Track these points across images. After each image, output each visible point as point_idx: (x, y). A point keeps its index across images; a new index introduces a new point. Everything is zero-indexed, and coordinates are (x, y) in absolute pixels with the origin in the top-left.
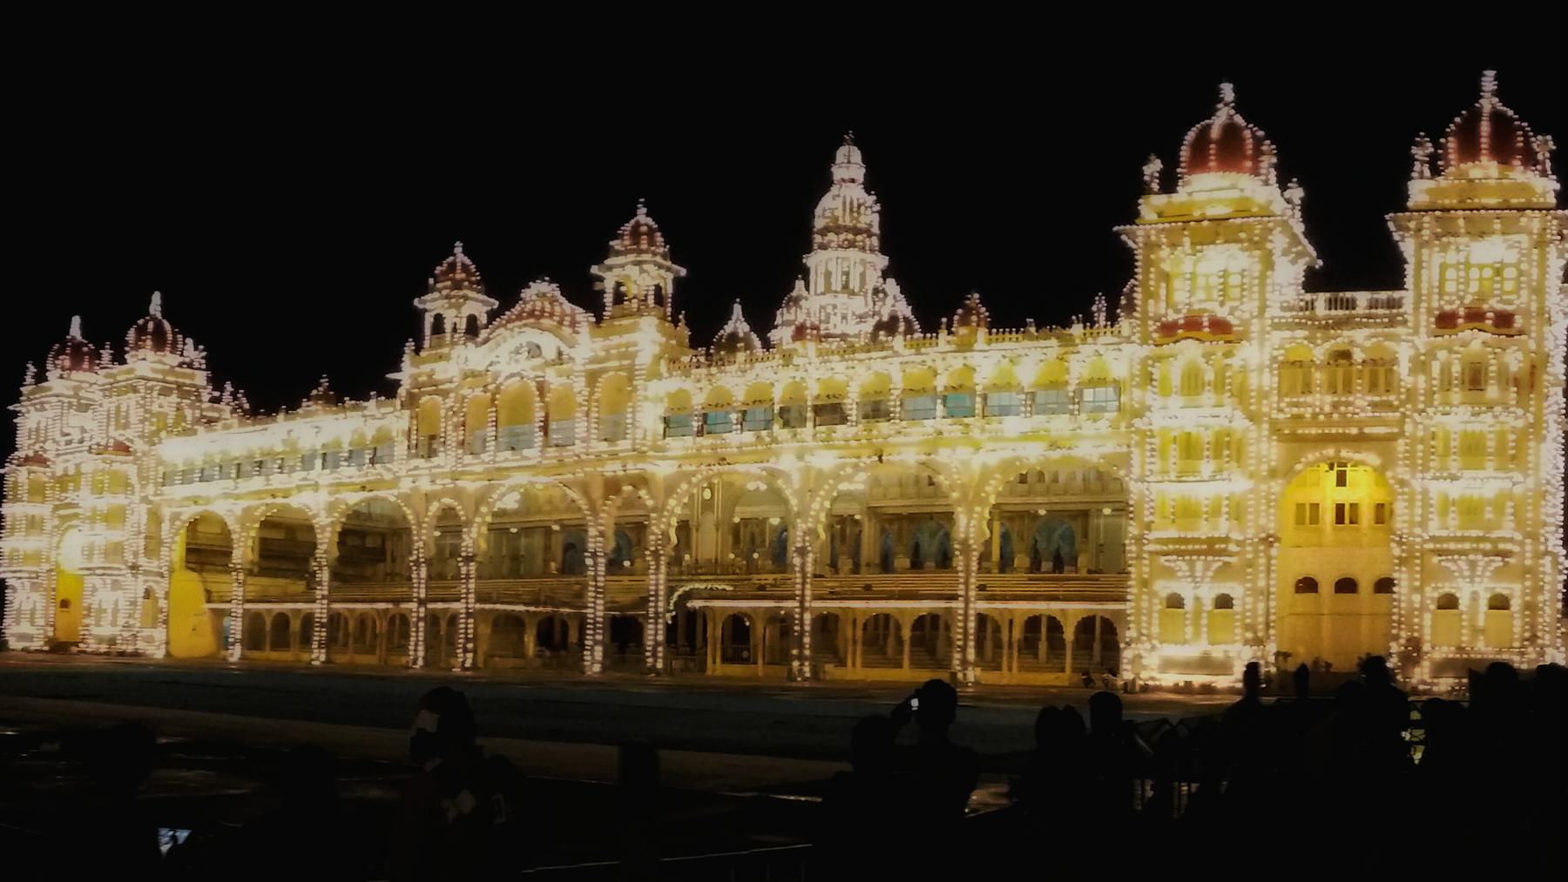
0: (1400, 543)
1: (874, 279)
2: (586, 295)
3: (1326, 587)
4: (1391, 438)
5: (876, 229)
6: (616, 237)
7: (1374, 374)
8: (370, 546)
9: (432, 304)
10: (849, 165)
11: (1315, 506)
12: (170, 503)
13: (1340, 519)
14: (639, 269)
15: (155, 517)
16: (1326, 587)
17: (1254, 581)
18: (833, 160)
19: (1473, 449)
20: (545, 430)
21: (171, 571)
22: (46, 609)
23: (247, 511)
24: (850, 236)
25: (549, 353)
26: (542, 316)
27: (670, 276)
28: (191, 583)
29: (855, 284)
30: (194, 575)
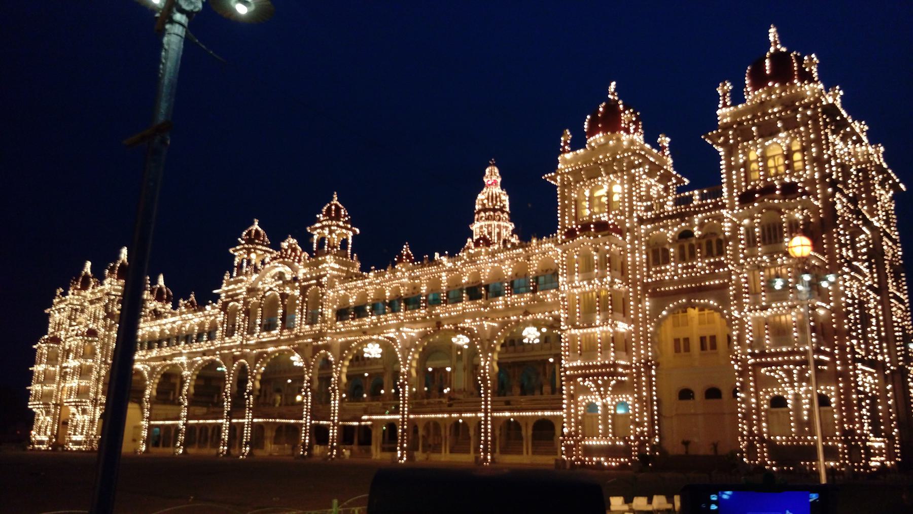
0: (736, 361)
4: (725, 286)
7: (709, 243)
9: (238, 255)
10: (492, 176)
11: (687, 340)
13: (703, 347)
14: (334, 229)
16: (699, 395)
17: (639, 392)
24: (492, 213)
25: (288, 277)
27: (351, 234)
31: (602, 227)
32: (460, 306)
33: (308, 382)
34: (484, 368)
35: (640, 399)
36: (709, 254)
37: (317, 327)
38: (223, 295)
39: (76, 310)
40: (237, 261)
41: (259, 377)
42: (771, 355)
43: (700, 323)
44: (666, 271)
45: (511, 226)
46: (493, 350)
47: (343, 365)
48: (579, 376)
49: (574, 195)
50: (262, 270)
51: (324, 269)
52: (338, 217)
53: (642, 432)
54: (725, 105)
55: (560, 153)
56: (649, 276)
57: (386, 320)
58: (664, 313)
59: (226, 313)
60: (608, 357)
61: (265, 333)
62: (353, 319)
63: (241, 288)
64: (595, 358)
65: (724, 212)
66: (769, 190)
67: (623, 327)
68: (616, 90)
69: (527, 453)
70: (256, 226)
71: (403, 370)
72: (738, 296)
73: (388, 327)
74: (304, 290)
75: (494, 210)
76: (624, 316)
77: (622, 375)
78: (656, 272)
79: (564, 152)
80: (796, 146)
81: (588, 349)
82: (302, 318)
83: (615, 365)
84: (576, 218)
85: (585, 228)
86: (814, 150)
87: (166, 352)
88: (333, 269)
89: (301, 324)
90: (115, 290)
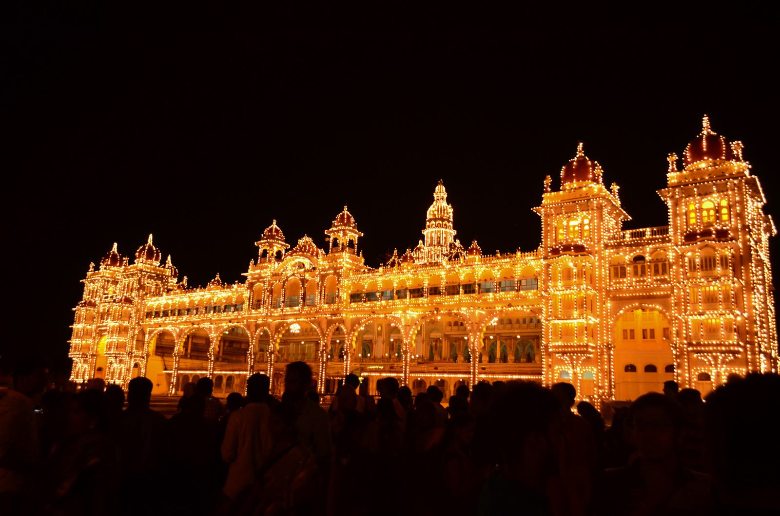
0: (675, 348)
1: (450, 240)
2: (322, 243)
3: (640, 369)
4: (668, 296)
6: (335, 219)
8: (233, 347)
9: (262, 246)
10: (440, 192)
11: (632, 331)
12: (150, 326)
14: (344, 232)
15: (143, 333)
16: (640, 369)
18: (434, 191)
19: (711, 300)
20: (304, 299)
21: (148, 355)
22: (90, 371)
23: (181, 330)
24: (441, 222)
26: (305, 251)
27: (357, 236)
28: (156, 362)
29: (442, 242)
30: (159, 358)
31: (579, 249)
32: (457, 297)
33: (324, 346)
34: (473, 343)
35: (602, 370)
36: (656, 272)
37: (334, 306)
38: (249, 277)
39: (108, 281)
40: (260, 251)
41: (278, 341)
42: (705, 345)
43: (643, 319)
44: (624, 282)
45: (454, 233)
46: (481, 331)
47: (354, 335)
48: (558, 353)
49: (555, 224)
51: (340, 263)
52: (348, 223)
53: (603, 393)
54: (673, 170)
55: (544, 192)
56: (610, 286)
57: (394, 304)
58: (621, 312)
60: (582, 340)
61: (288, 308)
62: (365, 302)
63: (266, 273)
64: (573, 341)
66: (706, 234)
67: (593, 320)
68: (583, 149)
70: (274, 226)
71: (405, 341)
73: (397, 309)
74: (323, 277)
75: (443, 220)
76: (592, 312)
77: (590, 353)
78: (616, 283)
79: (547, 191)
81: (567, 333)
82: (320, 299)
83: (587, 346)
84: (556, 240)
85: (567, 248)
86: (738, 208)
87: (195, 318)
88: (347, 263)
89: (320, 303)
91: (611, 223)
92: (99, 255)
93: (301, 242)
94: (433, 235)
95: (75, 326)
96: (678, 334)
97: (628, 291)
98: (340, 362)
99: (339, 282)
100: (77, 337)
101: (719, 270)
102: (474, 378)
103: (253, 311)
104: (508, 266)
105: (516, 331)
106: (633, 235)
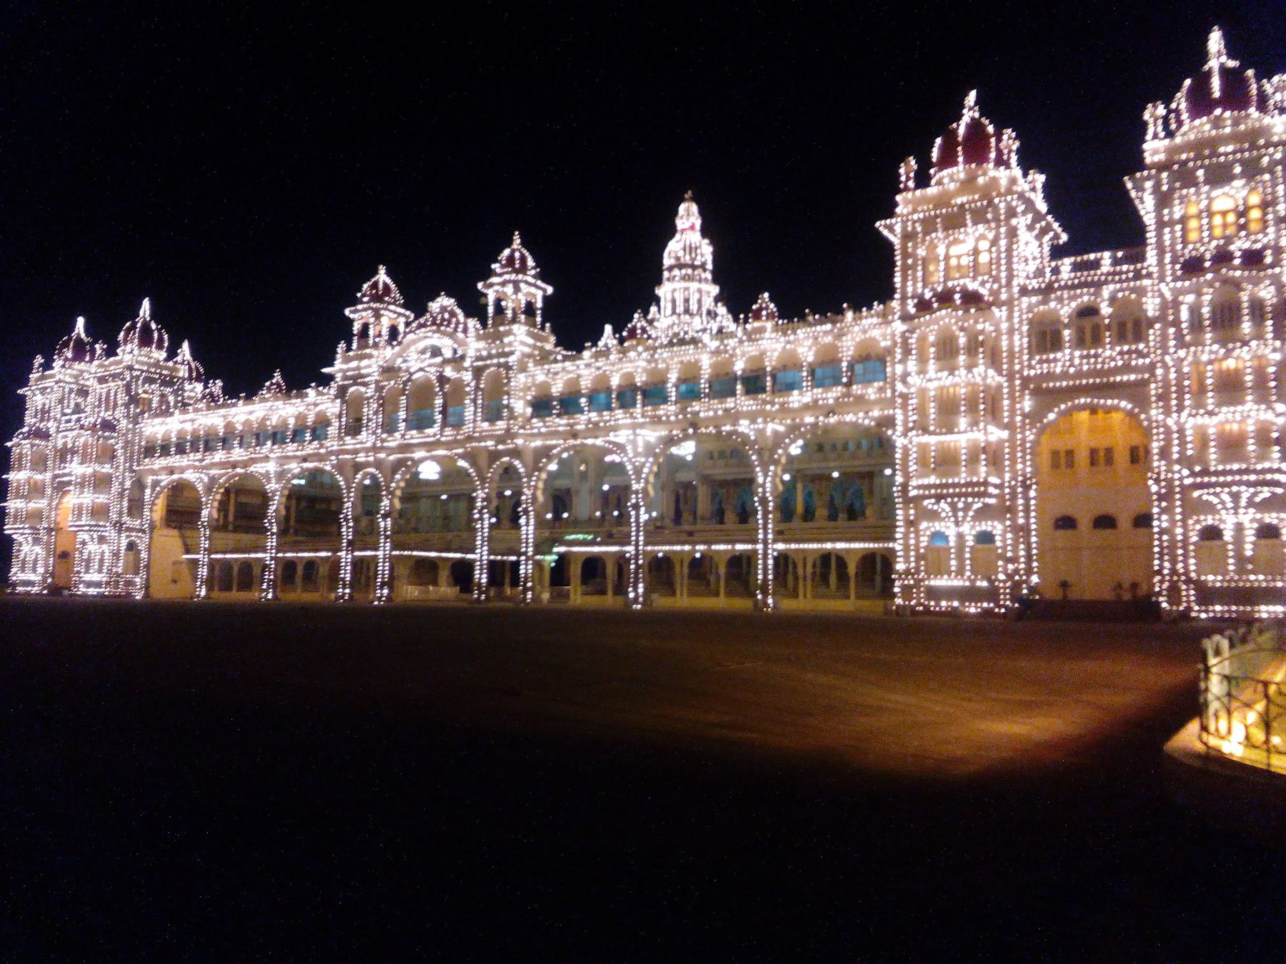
0: (1157, 481)
1: (708, 303)
2: (473, 306)
4: (1144, 384)
5: (710, 266)
6: (496, 261)
9: (358, 315)
10: (688, 216)
11: (1070, 453)
12: (154, 472)
13: (1093, 462)
15: (139, 485)
17: (1013, 519)
18: (676, 213)
19: (1230, 388)
20: (444, 412)
21: (152, 527)
22: (46, 559)
23: (213, 480)
24: (690, 271)
26: (441, 324)
28: (170, 540)
29: (694, 307)
30: (175, 532)
31: (972, 299)
32: (730, 403)
33: (484, 499)
34: (763, 485)
35: (1016, 529)
36: (1121, 338)
37: (501, 425)
38: (339, 376)
40: (356, 327)
41: (398, 493)
42: (1216, 473)
43: (1092, 430)
44: (1055, 360)
46: (776, 463)
47: (539, 478)
48: (929, 497)
49: (921, 252)
50: (397, 342)
51: (510, 344)
52: (523, 269)
53: (1016, 571)
55: (899, 191)
56: (1030, 367)
58: (1052, 416)
59: (343, 402)
60: (975, 473)
61: (414, 432)
62: (559, 415)
63: (369, 366)
64: (957, 474)
65: (1146, 282)
67: (996, 434)
68: (976, 103)
69: (805, 596)
70: (382, 277)
71: (635, 487)
72: (1164, 397)
74: (478, 372)
75: (694, 267)
77: (991, 496)
78: (1041, 362)
79: (907, 189)
80: (1255, 199)
81: (946, 461)
82: (475, 413)
83: (986, 483)
88: (523, 343)
89: (475, 421)
90: (138, 362)
91: (1031, 249)
92: (48, 340)
93: (434, 306)
94: (677, 295)
95: (12, 476)
96: (1165, 453)
97: (1065, 375)
98: (513, 528)
99: (509, 379)
100: (17, 497)
101: (1246, 327)
102: (766, 549)
103: (348, 438)
104: (829, 339)
105: (832, 464)
106: (1076, 267)
